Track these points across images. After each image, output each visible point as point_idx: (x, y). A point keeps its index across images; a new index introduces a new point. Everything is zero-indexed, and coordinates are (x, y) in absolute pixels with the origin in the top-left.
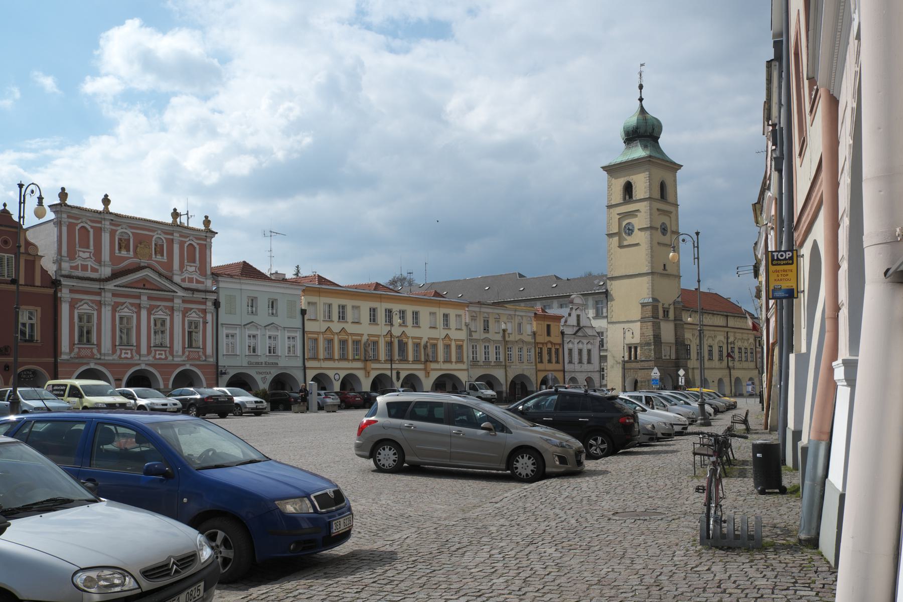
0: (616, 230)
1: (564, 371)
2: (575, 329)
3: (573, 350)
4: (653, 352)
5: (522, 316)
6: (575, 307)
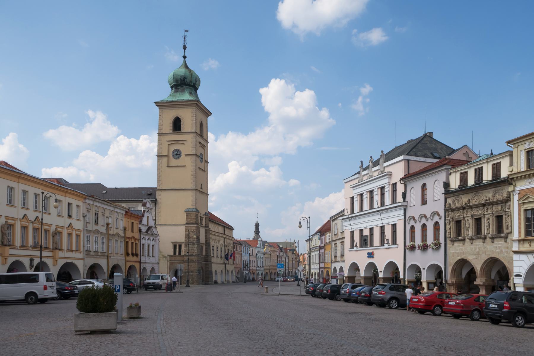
0: (166, 154)
1: (140, 263)
2: (147, 228)
3: (145, 245)
4: (196, 250)
5: (118, 213)
6: (147, 210)
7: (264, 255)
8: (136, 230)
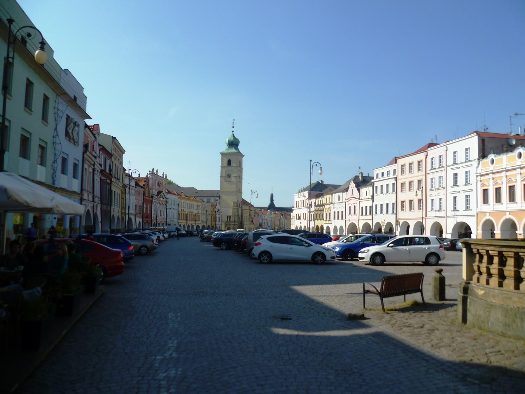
1: (216, 224)
2: (217, 210)
7: (271, 219)
8: (214, 211)
